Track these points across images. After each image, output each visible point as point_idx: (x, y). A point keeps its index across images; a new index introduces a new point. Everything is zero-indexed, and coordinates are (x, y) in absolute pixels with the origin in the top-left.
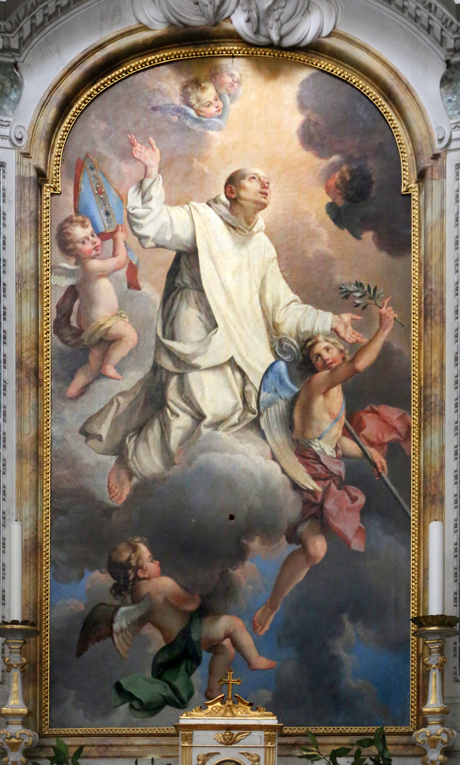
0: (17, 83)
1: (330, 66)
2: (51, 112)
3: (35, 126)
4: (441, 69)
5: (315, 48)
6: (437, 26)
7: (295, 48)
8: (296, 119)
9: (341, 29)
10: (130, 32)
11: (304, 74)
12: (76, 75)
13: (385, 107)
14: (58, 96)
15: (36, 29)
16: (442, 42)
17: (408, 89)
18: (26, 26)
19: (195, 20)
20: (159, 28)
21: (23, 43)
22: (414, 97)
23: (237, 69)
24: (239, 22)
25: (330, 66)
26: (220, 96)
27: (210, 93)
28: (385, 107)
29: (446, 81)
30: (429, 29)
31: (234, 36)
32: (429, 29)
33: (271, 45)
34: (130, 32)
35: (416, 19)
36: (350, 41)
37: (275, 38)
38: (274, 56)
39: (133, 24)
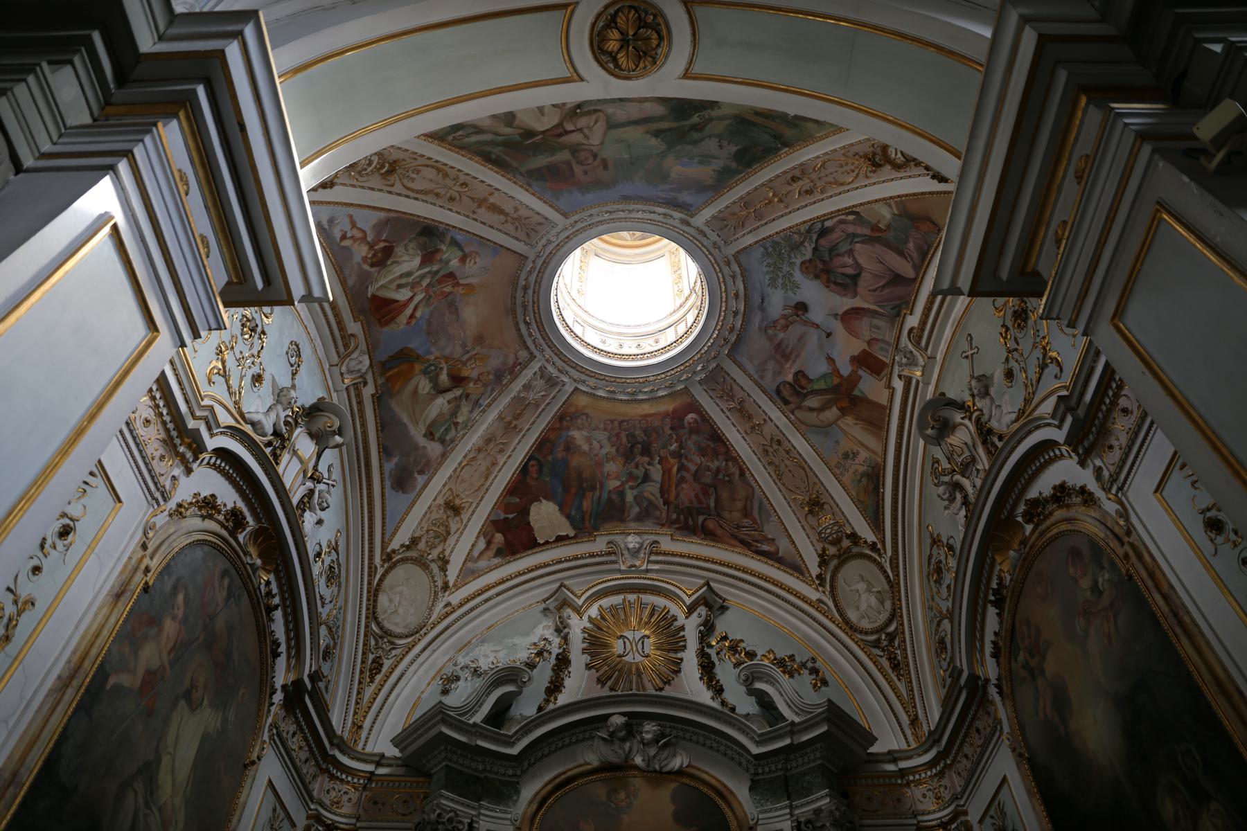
0: (518, 792)
1: (687, 781)
2: (535, 806)
3: (525, 813)
4: (749, 784)
5: (680, 772)
6: (744, 763)
7: (670, 773)
8: (670, 809)
9: (693, 763)
10: (580, 766)
11: (674, 785)
12: (549, 787)
13: (720, 802)
14: (539, 797)
15: (530, 765)
16: (747, 770)
17: (731, 792)
18: (526, 764)
19: (614, 759)
20: (596, 764)
21: (523, 772)
22: (735, 797)
23: (638, 782)
24: (638, 760)
25: (687, 781)
26: (628, 797)
27: (623, 795)
28: (720, 802)
29: (751, 789)
30: (740, 764)
31: (636, 767)
32: (740, 764)
33: (655, 771)
34: (580, 766)
35: (733, 759)
36: (699, 769)
37: (657, 767)
38: (657, 776)
39: (582, 762)
